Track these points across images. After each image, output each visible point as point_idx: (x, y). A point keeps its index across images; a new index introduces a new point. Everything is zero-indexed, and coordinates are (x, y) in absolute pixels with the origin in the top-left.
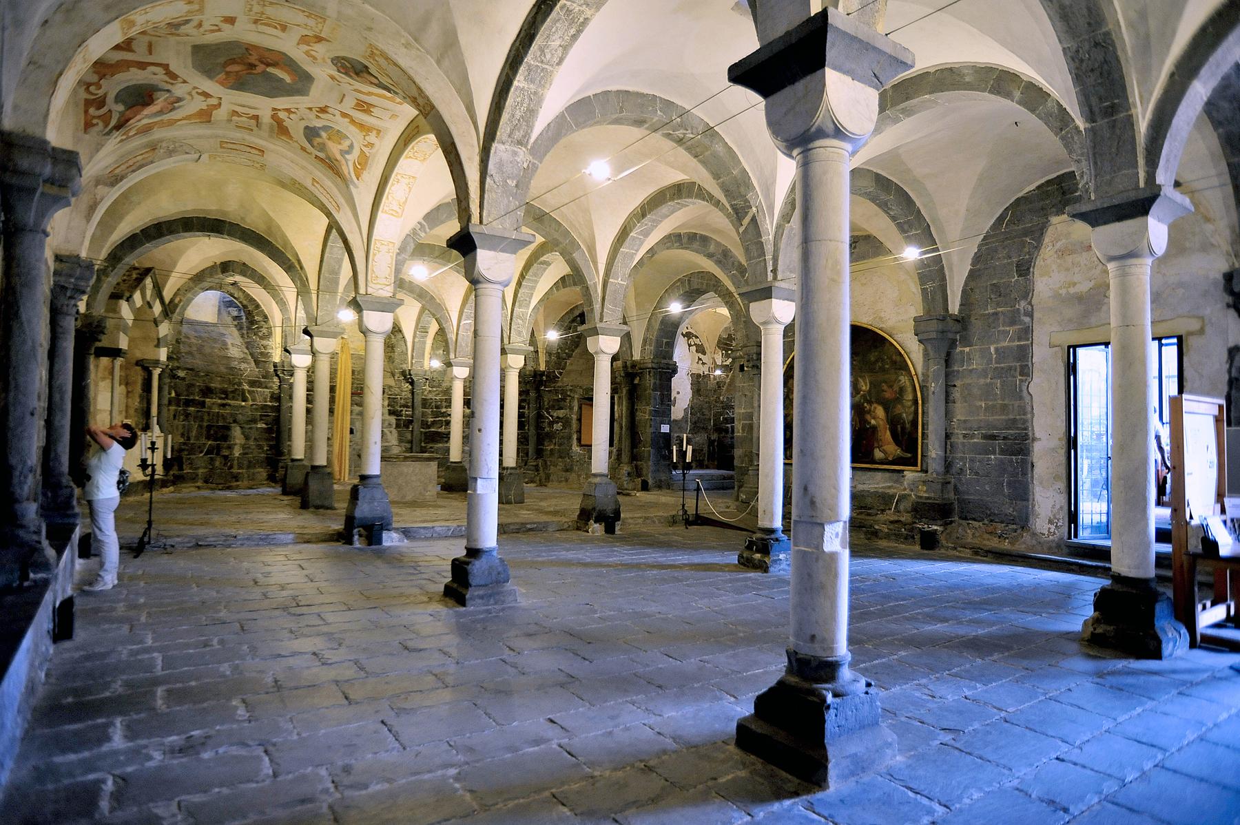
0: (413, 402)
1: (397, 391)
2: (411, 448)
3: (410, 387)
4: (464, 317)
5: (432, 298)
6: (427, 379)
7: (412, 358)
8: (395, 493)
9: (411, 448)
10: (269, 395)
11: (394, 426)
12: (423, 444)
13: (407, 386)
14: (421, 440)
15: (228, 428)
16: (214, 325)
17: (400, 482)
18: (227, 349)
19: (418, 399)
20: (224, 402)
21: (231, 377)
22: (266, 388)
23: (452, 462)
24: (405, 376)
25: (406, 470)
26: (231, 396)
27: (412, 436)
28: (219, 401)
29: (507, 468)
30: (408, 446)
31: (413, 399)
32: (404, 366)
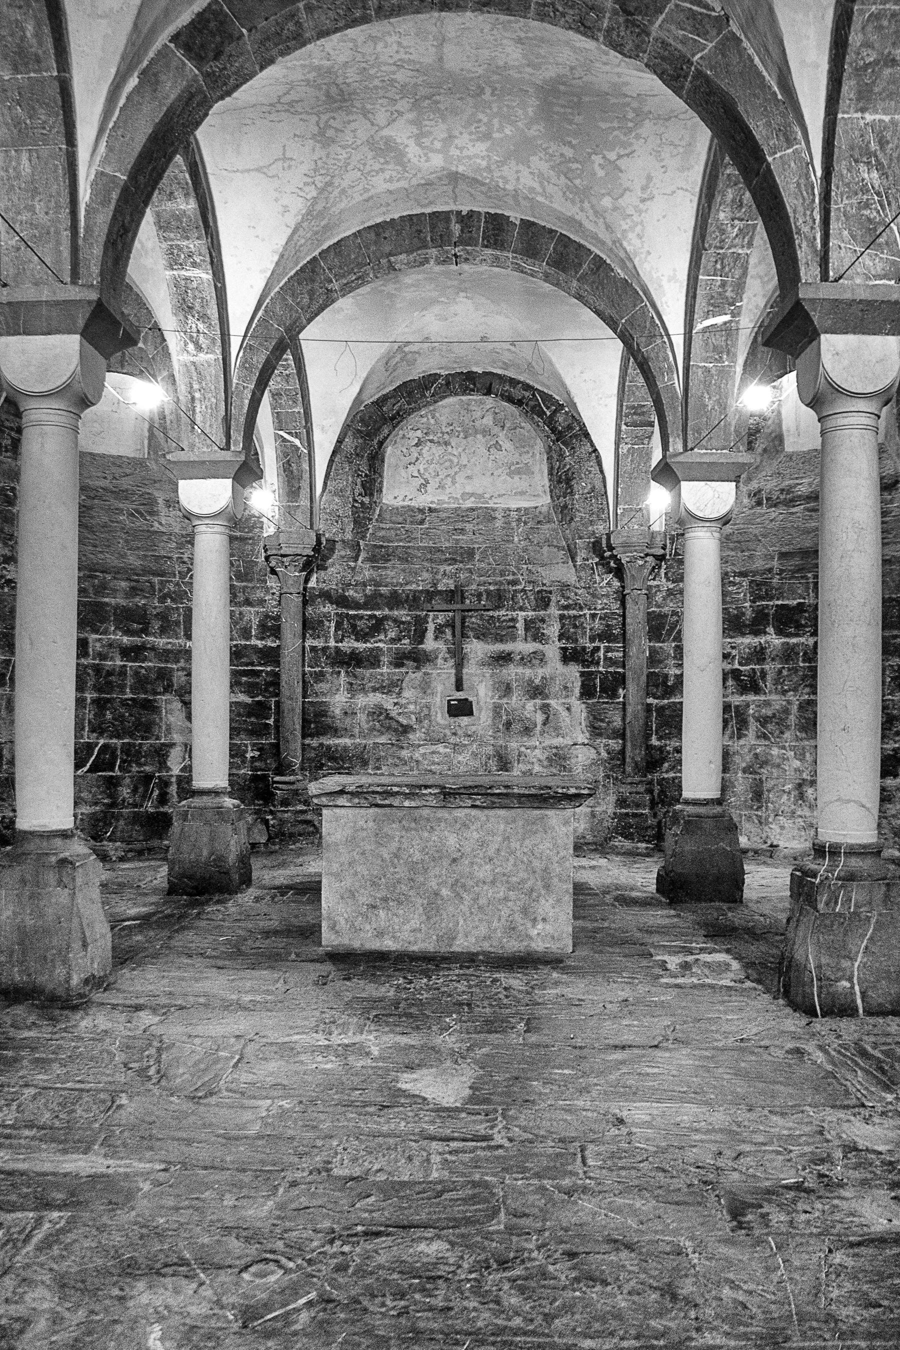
0: (624, 624)
1: (583, 595)
2: (623, 752)
3: (616, 583)
4: (701, 304)
5: (599, 263)
6: (661, 558)
7: (617, 504)
8: (415, 923)
9: (623, 752)
10: (255, 622)
11: (577, 691)
12: (654, 741)
13: (606, 582)
14: (647, 726)
15: (150, 706)
16: (139, 463)
17: (433, 884)
18: (152, 513)
19: (636, 615)
20: (137, 640)
21: (156, 580)
22: (247, 602)
23: (687, 802)
24: (602, 558)
25: (452, 840)
26: (156, 625)
27: (624, 719)
28: (125, 639)
29: (834, 851)
30: (615, 744)
31: (624, 616)
32: (600, 528)
